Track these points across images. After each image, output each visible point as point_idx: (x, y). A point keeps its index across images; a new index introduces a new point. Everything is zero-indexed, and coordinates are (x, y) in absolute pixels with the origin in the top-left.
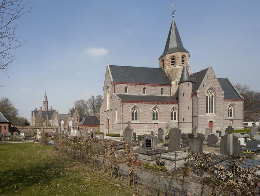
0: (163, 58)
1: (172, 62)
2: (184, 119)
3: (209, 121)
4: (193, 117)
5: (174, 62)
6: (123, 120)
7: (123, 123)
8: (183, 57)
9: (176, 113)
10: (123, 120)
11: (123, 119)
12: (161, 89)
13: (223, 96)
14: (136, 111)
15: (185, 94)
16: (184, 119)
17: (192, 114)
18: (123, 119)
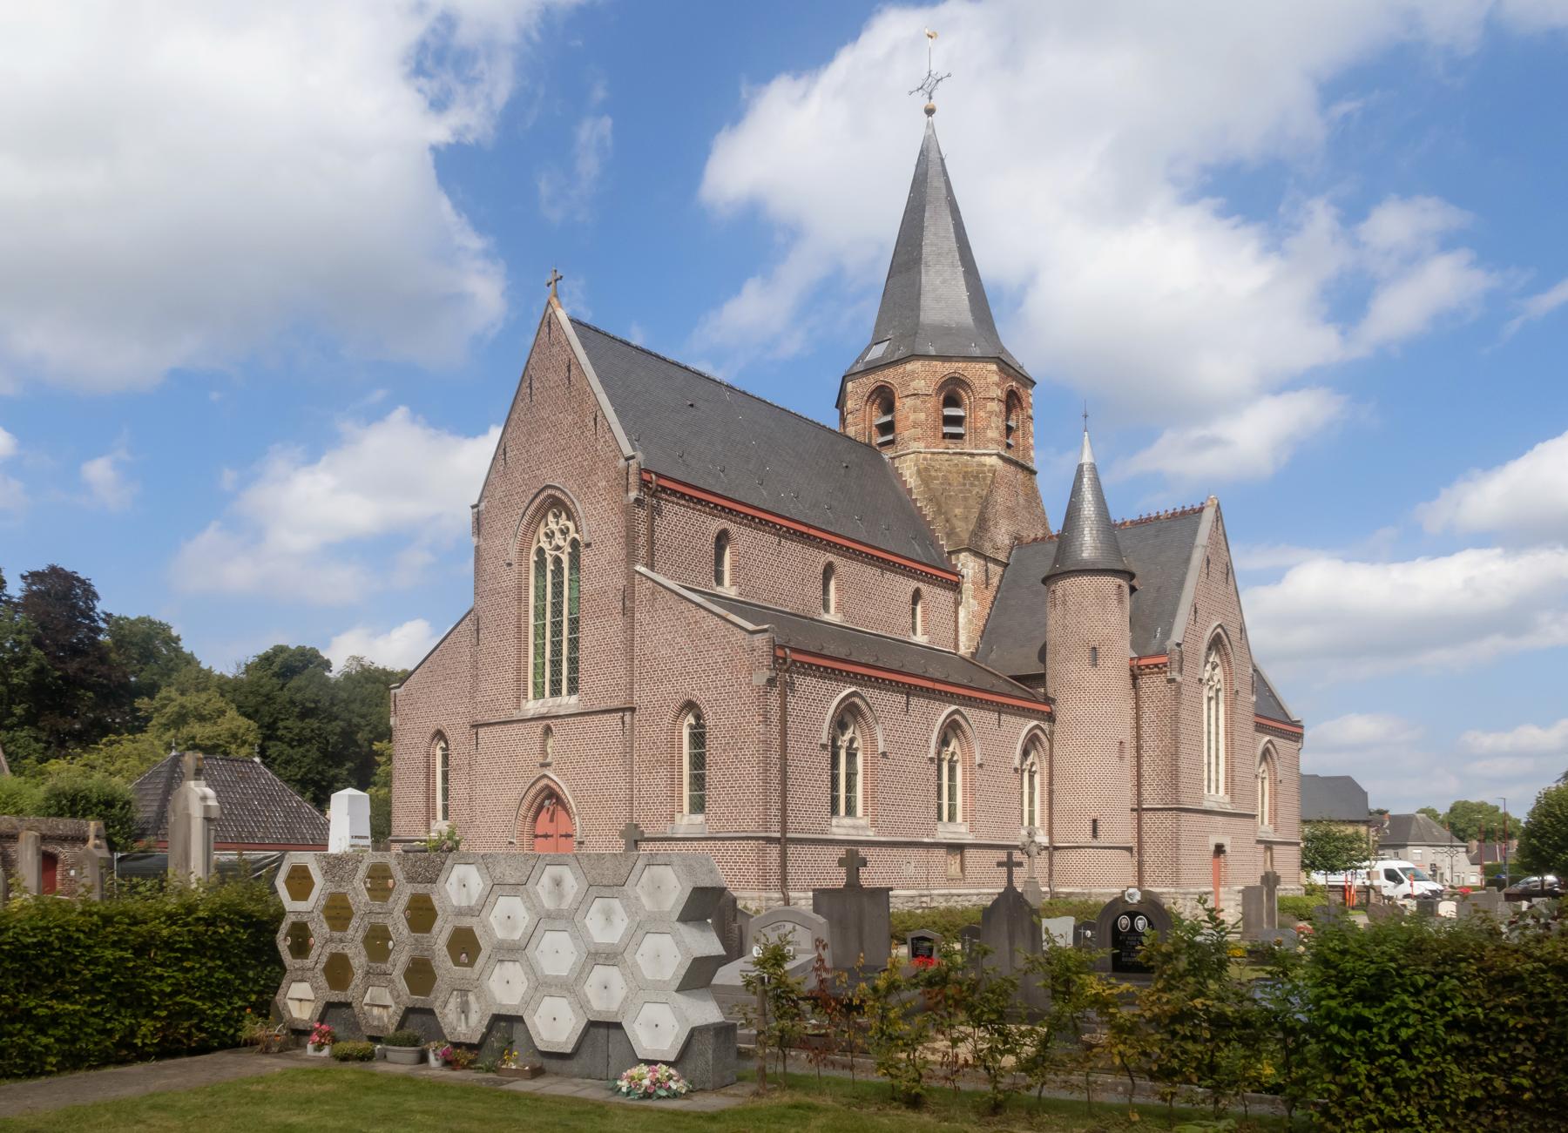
0: (890, 376)
1: (949, 421)
2: (1095, 821)
3: (1213, 840)
4: (1139, 810)
5: (957, 421)
6: (784, 810)
7: (784, 829)
8: (1012, 401)
9: (1037, 778)
10: (784, 810)
11: (784, 796)
12: (910, 591)
13: (1254, 698)
14: (852, 741)
15: (1102, 651)
16: (1095, 821)
17: (1139, 794)
18: (784, 796)
